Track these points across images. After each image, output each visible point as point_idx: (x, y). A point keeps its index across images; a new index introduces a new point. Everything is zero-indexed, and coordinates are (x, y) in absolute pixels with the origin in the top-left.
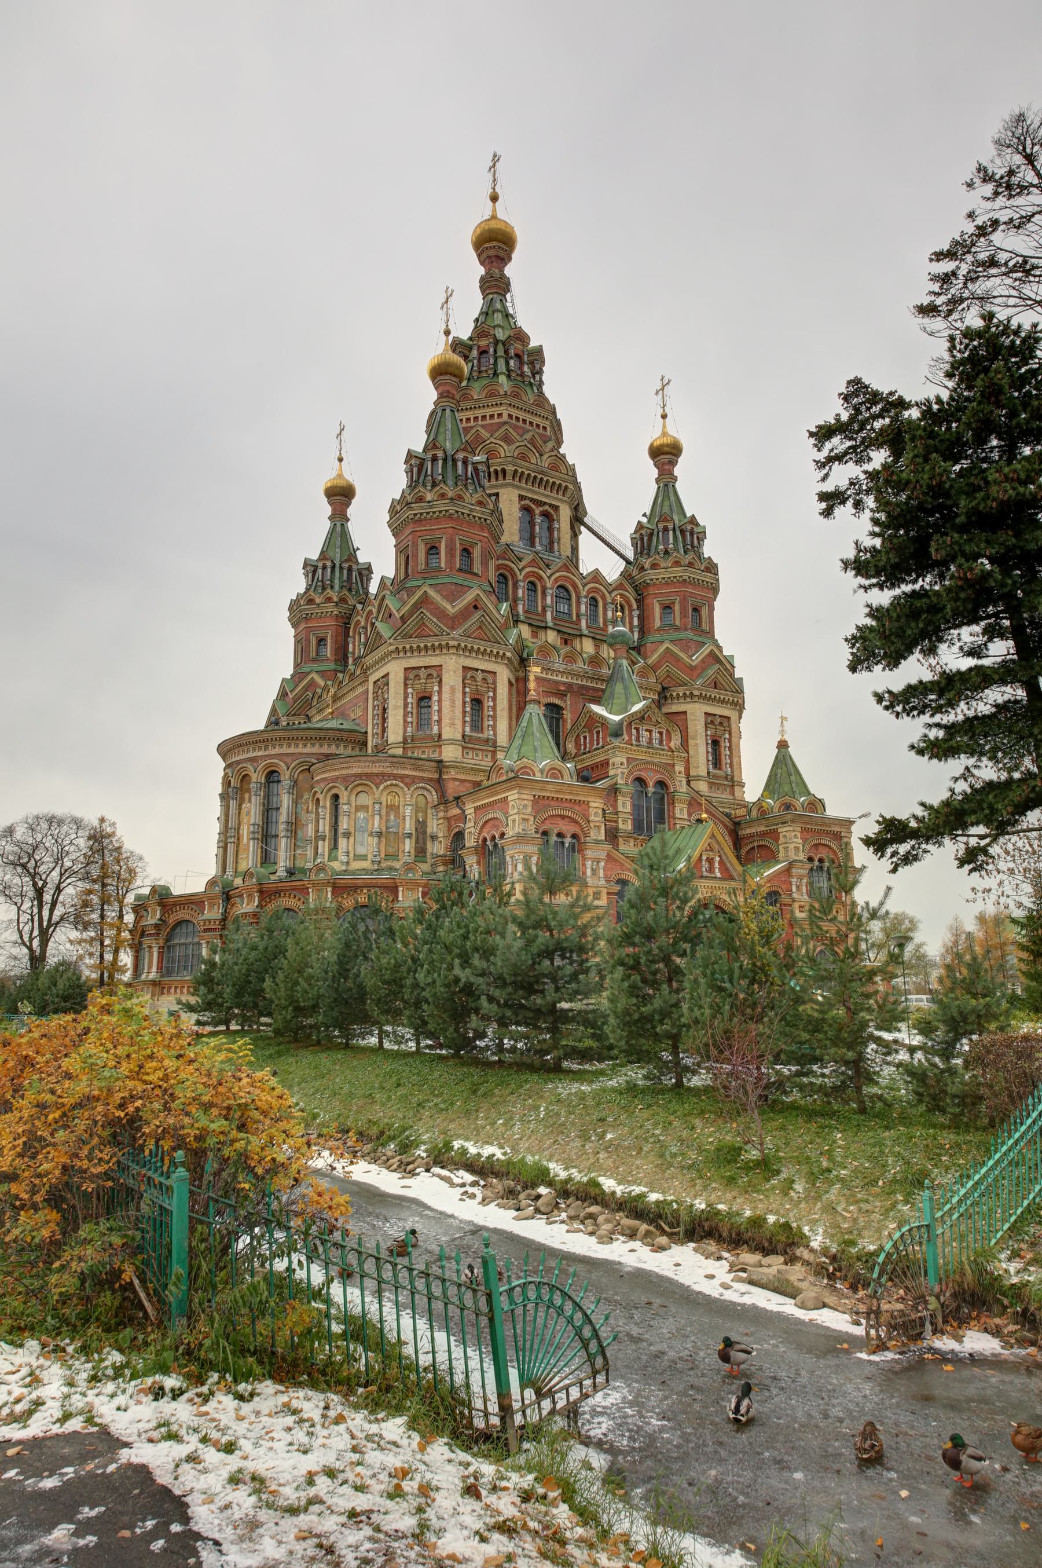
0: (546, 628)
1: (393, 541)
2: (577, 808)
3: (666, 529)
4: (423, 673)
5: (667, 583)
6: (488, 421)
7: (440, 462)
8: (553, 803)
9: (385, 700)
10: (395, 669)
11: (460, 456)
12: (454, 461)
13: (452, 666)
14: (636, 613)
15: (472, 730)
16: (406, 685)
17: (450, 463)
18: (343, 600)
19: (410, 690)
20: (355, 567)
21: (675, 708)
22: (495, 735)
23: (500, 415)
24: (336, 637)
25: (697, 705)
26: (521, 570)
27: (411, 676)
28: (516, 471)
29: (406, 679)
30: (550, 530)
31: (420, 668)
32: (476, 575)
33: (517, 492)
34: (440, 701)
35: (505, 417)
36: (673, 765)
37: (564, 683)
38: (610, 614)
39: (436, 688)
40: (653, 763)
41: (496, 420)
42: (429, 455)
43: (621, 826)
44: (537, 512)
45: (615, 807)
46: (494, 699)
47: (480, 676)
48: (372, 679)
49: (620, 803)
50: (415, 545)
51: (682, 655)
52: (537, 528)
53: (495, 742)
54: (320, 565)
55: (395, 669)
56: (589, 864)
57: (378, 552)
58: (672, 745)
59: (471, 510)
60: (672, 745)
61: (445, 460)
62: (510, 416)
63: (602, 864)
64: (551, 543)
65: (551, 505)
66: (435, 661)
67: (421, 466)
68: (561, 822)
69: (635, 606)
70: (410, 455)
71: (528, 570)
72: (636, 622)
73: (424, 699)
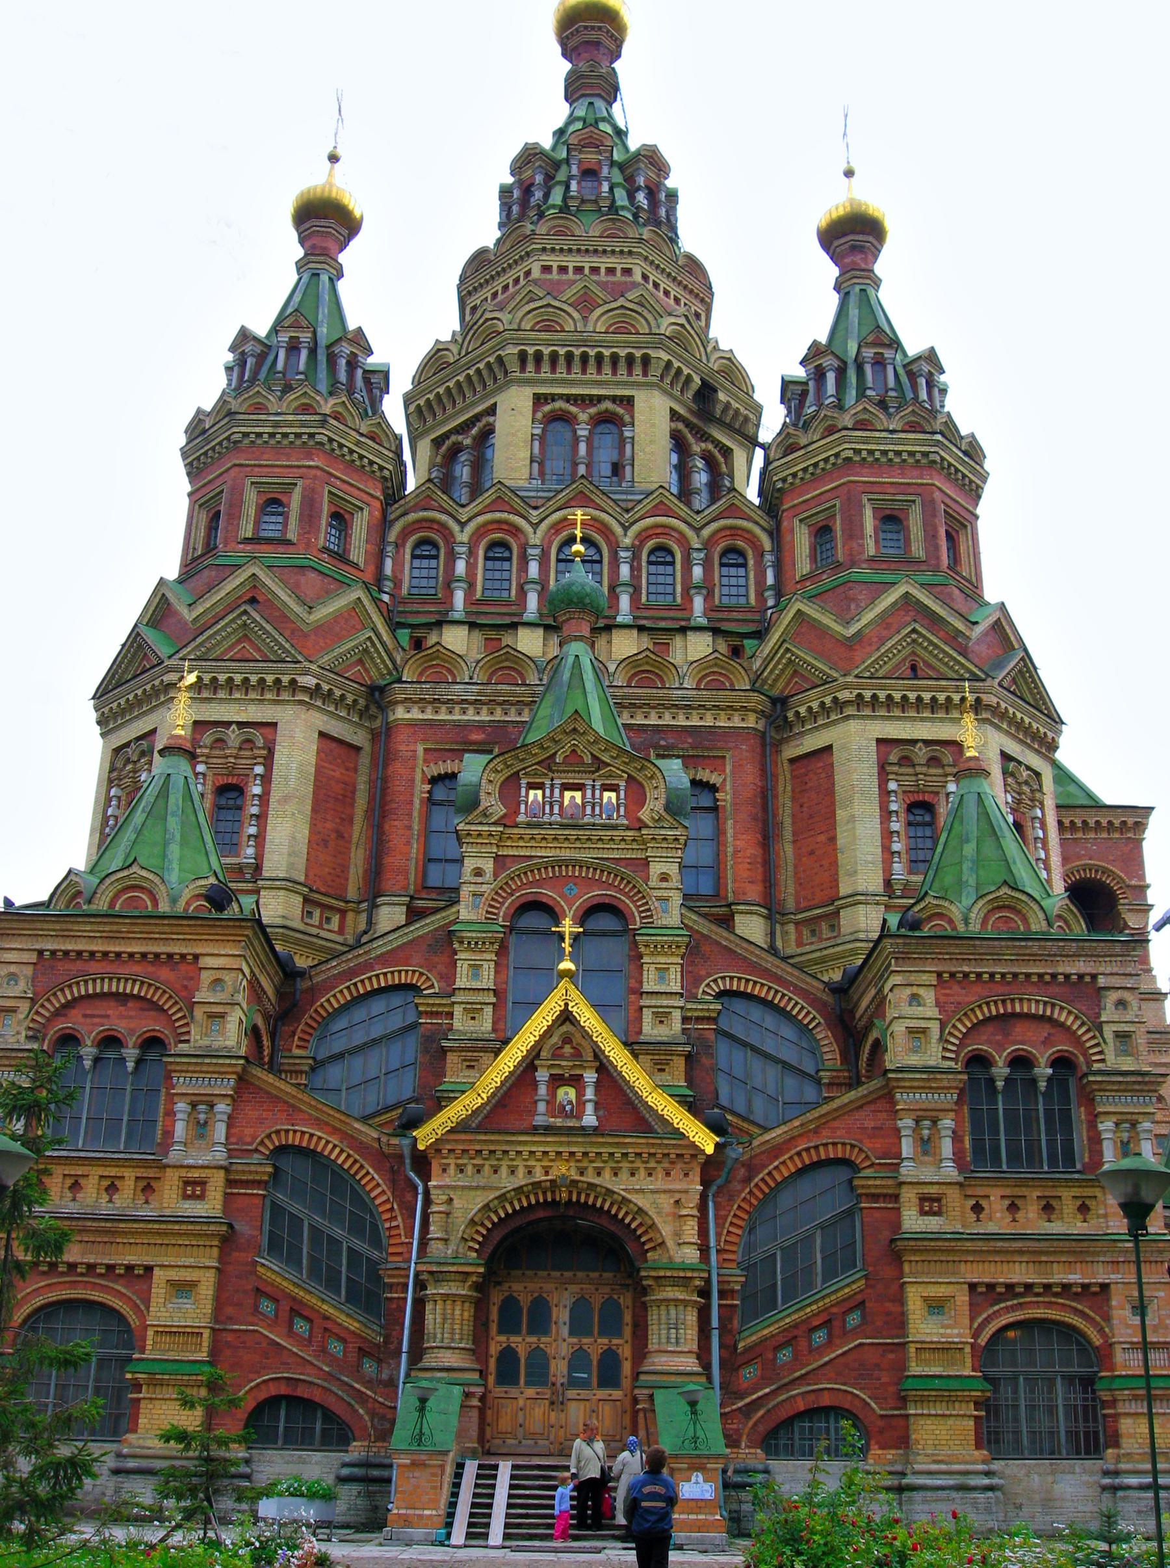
2: (165, 973)
5: (816, 475)
8: (94, 967)
14: (769, 558)
21: (811, 742)
22: (259, 856)
23: (528, 273)
25: (853, 726)
26: (462, 525)
28: (523, 356)
32: (289, 543)
33: (528, 392)
35: (536, 273)
36: (646, 862)
37: (480, 726)
38: (697, 572)
40: (575, 863)
43: (460, 1022)
44: (583, 417)
45: (449, 976)
46: (266, 779)
47: (233, 736)
49: (462, 968)
51: (827, 620)
53: (258, 868)
56: (181, 1106)
58: (644, 814)
59: (276, 424)
60: (644, 814)
62: (546, 269)
63: (222, 1107)
65: (614, 399)
68: (112, 1009)
69: (767, 544)
71: (480, 519)
72: (770, 580)
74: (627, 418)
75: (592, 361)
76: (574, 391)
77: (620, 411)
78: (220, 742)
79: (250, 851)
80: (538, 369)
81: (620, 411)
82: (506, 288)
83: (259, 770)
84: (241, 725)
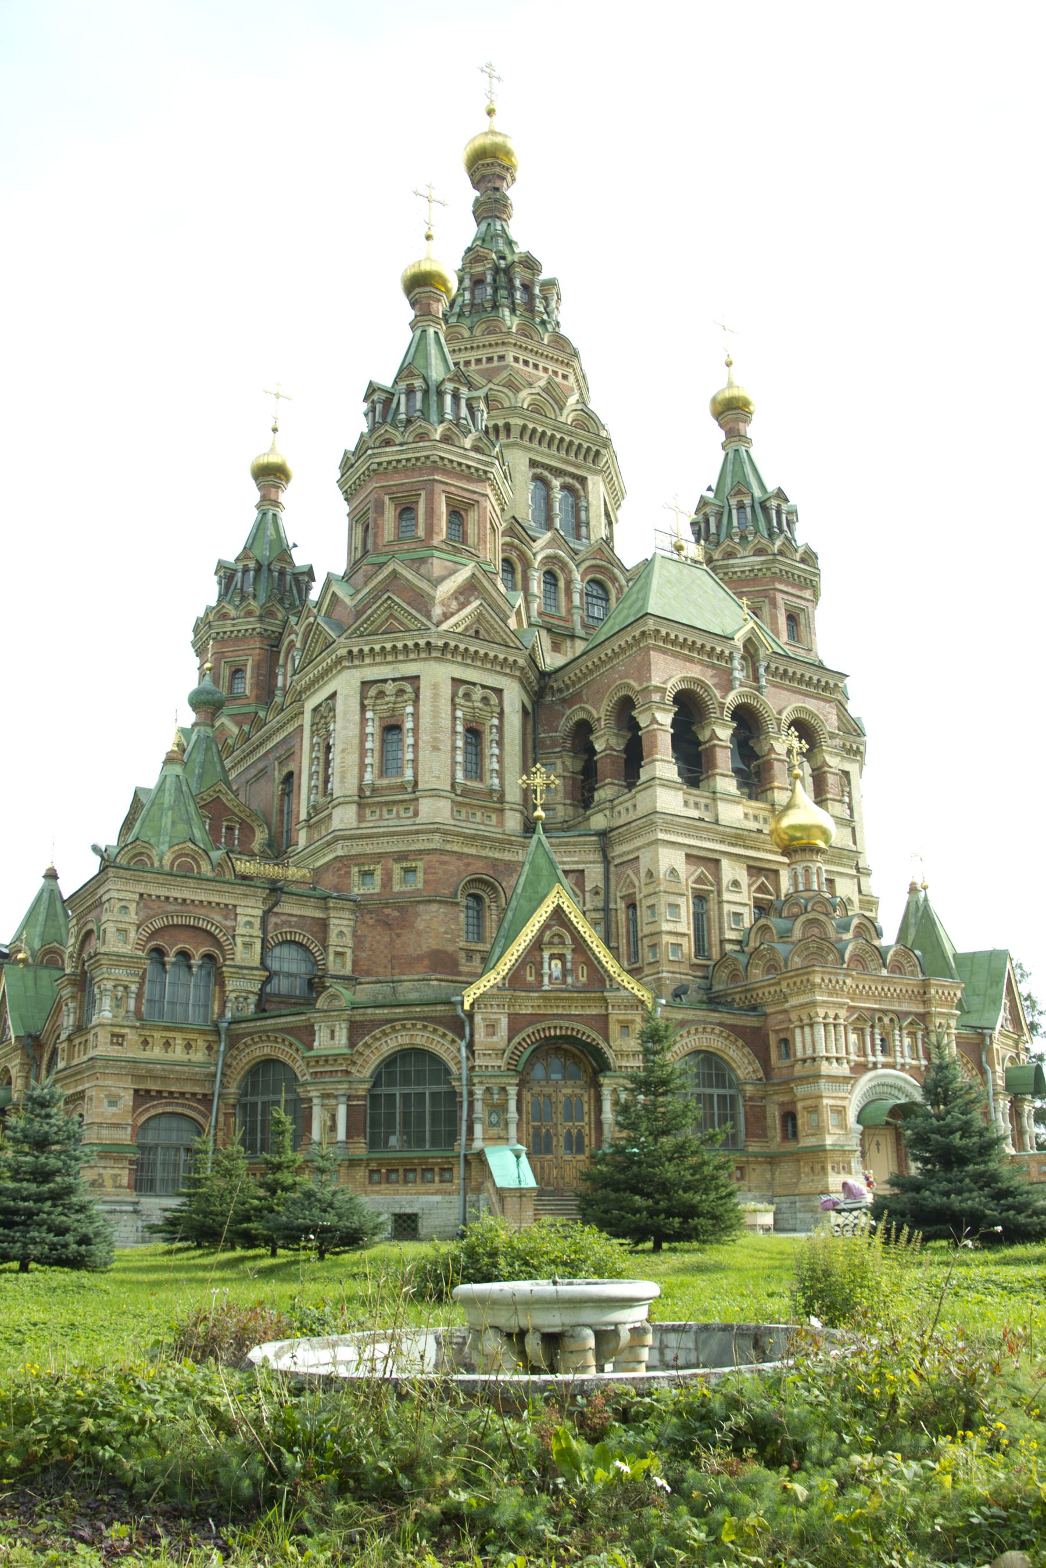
0: (573, 637)
1: (345, 508)
3: (741, 507)
4: (390, 688)
6: (484, 365)
7: (419, 396)
9: (329, 734)
10: (346, 685)
11: (449, 386)
12: (440, 394)
13: (436, 676)
15: (466, 777)
16: (363, 708)
17: (433, 398)
18: (267, 614)
19: (369, 715)
20: (289, 570)
23: (502, 358)
24: (257, 666)
27: (373, 692)
28: (524, 427)
29: (363, 697)
30: (576, 510)
31: (385, 681)
34: (415, 730)
39: (410, 709)
41: (495, 363)
42: (403, 385)
44: (556, 483)
46: (500, 729)
47: (478, 694)
48: (310, 705)
50: (379, 508)
52: (557, 506)
53: (502, 795)
54: (240, 566)
55: (346, 685)
57: (320, 538)
61: (426, 392)
64: (578, 526)
66: (409, 669)
67: (387, 403)
70: (373, 389)
73: (392, 729)
74: (582, 493)
75: (565, 444)
76: (553, 463)
77: (578, 486)
78: (467, 696)
79: (496, 781)
80: (531, 440)
81: (578, 486)
82: (479, 361)
83: (496, 722)
84: (483, 687)
